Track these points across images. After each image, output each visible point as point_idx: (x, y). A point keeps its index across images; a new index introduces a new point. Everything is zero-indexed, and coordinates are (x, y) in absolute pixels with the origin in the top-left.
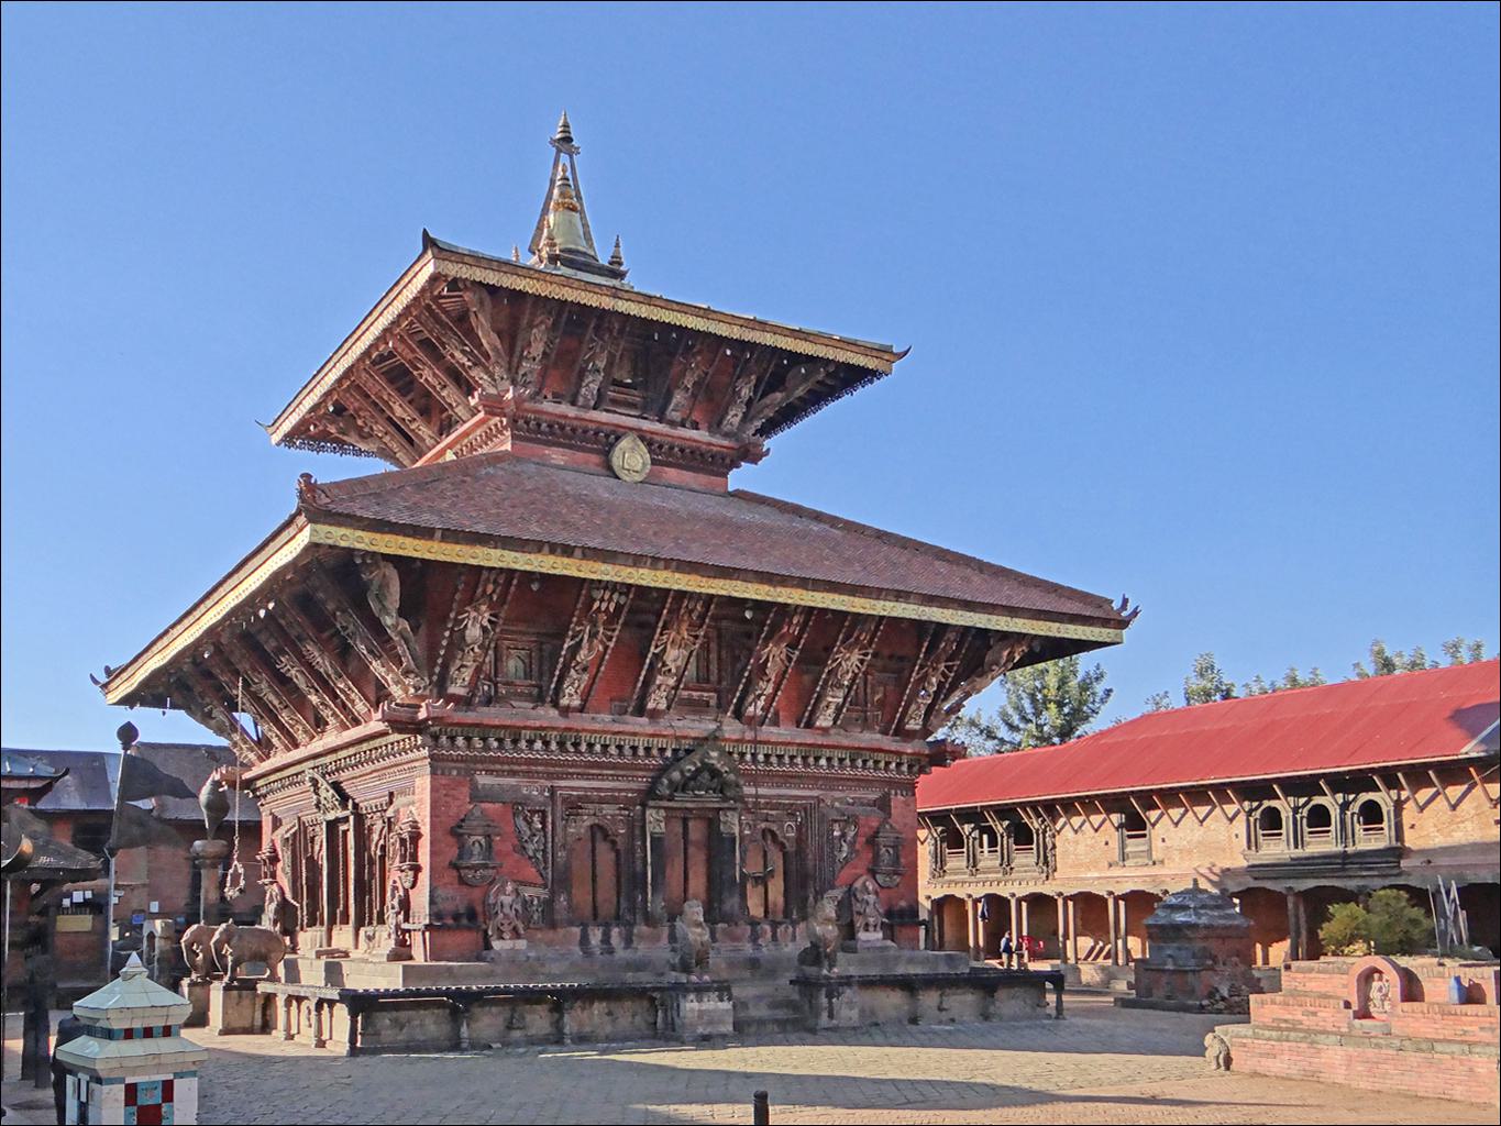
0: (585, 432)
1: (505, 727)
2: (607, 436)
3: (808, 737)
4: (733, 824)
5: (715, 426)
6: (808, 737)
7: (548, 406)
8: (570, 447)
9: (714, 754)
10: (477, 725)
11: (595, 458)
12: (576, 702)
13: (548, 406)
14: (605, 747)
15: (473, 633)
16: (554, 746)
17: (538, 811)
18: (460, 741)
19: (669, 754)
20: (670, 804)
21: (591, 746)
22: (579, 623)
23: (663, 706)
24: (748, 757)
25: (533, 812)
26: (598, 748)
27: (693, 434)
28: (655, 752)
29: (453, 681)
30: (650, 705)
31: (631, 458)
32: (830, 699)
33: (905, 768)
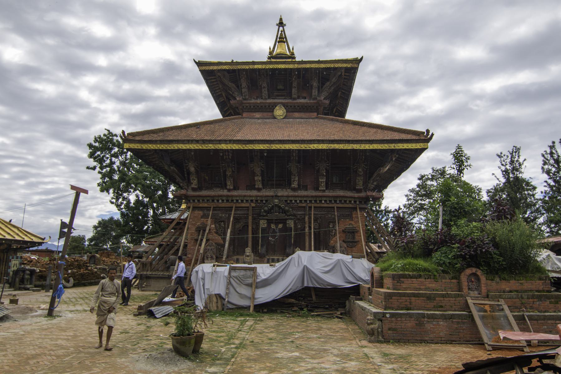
0: (265, 106)
1: (209, 196)
2: (273, 106)
3: (314, 193)
4: (291, 223)
5: (310, 96)
6: (314, 193)
7: (253, 101)
8: (262, 111)
9: (277, 201)
11: (270, 114)
12: (232, 188)
13: (253, 101)
14: (242, 201)
16: (225, 201)
17: (223, 221)
18: (196, 201)
19: (264, 202)
20: (267, 218)
21: (237, 201)
22: (222, 163)
23: (261, 186)
24: (293, 201)
25: (221, 222)
26: (240, 201)
27: (302, 101)
28: (259, 201)
29: (192, 183)
30: (256, 186)
31: (279, 112)
33: (358, 203)
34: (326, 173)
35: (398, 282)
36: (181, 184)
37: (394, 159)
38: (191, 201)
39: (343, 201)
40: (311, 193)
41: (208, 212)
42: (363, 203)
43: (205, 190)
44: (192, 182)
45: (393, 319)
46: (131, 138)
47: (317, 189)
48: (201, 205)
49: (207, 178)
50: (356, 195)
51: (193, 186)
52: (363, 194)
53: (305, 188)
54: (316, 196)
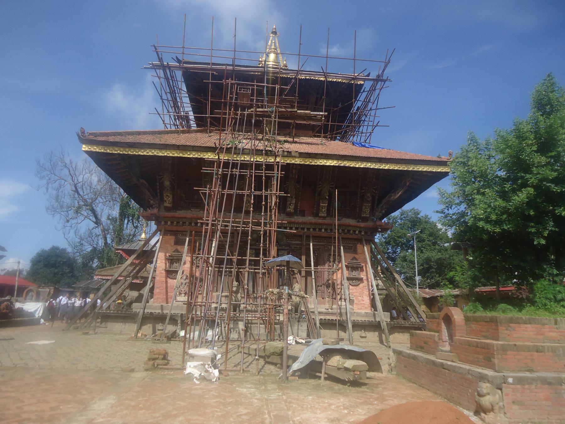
1: (185, 218)
10: (175, 217)
15: (167, 183)
32: (322, 205)
33: (363, 233)
34: (328, 196)
35: (507, 330)
36: (152, 202)
37: (408, 184)
38: (163, 223)
39: (346, 231)
40: (309, 219)
41: (184, 238)
42: (369, 233)
43: (181, 210)
44: (165, 199)
45: (519, 386)
46: (91, 137)
47: (316, 215)
48: (174, 228)
49: (184, 196)
50: (362, 225)
51: (167, 204)
52: (370, 224)
53: (303, 214)
54: (315, 224)
